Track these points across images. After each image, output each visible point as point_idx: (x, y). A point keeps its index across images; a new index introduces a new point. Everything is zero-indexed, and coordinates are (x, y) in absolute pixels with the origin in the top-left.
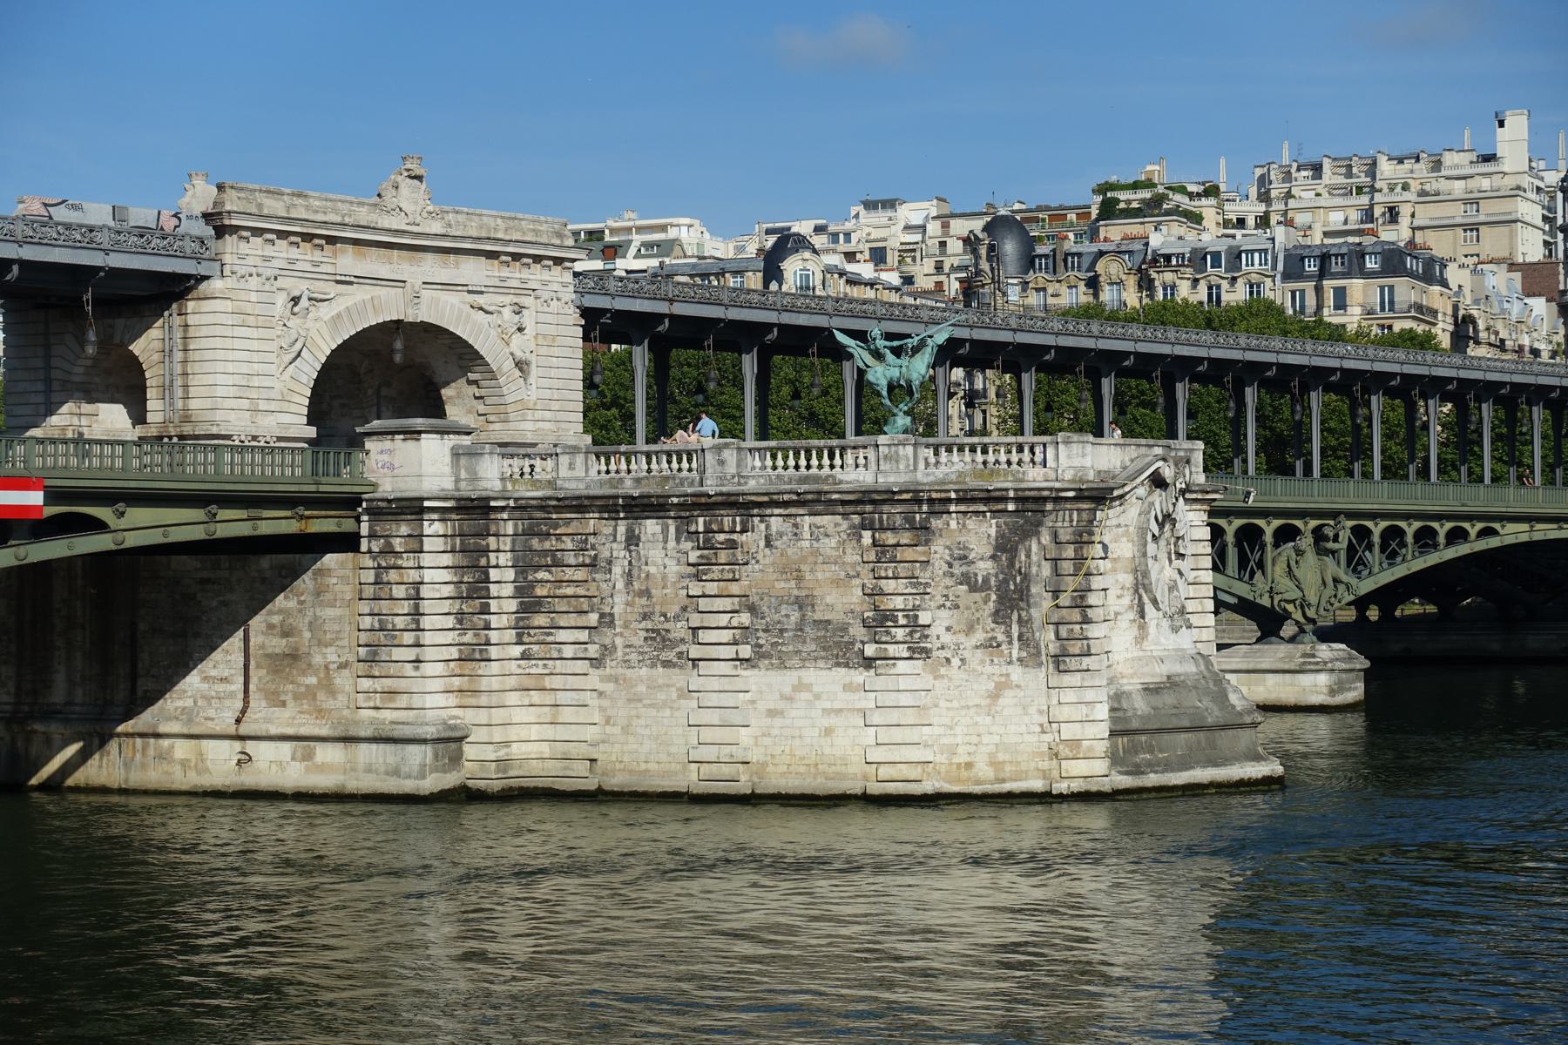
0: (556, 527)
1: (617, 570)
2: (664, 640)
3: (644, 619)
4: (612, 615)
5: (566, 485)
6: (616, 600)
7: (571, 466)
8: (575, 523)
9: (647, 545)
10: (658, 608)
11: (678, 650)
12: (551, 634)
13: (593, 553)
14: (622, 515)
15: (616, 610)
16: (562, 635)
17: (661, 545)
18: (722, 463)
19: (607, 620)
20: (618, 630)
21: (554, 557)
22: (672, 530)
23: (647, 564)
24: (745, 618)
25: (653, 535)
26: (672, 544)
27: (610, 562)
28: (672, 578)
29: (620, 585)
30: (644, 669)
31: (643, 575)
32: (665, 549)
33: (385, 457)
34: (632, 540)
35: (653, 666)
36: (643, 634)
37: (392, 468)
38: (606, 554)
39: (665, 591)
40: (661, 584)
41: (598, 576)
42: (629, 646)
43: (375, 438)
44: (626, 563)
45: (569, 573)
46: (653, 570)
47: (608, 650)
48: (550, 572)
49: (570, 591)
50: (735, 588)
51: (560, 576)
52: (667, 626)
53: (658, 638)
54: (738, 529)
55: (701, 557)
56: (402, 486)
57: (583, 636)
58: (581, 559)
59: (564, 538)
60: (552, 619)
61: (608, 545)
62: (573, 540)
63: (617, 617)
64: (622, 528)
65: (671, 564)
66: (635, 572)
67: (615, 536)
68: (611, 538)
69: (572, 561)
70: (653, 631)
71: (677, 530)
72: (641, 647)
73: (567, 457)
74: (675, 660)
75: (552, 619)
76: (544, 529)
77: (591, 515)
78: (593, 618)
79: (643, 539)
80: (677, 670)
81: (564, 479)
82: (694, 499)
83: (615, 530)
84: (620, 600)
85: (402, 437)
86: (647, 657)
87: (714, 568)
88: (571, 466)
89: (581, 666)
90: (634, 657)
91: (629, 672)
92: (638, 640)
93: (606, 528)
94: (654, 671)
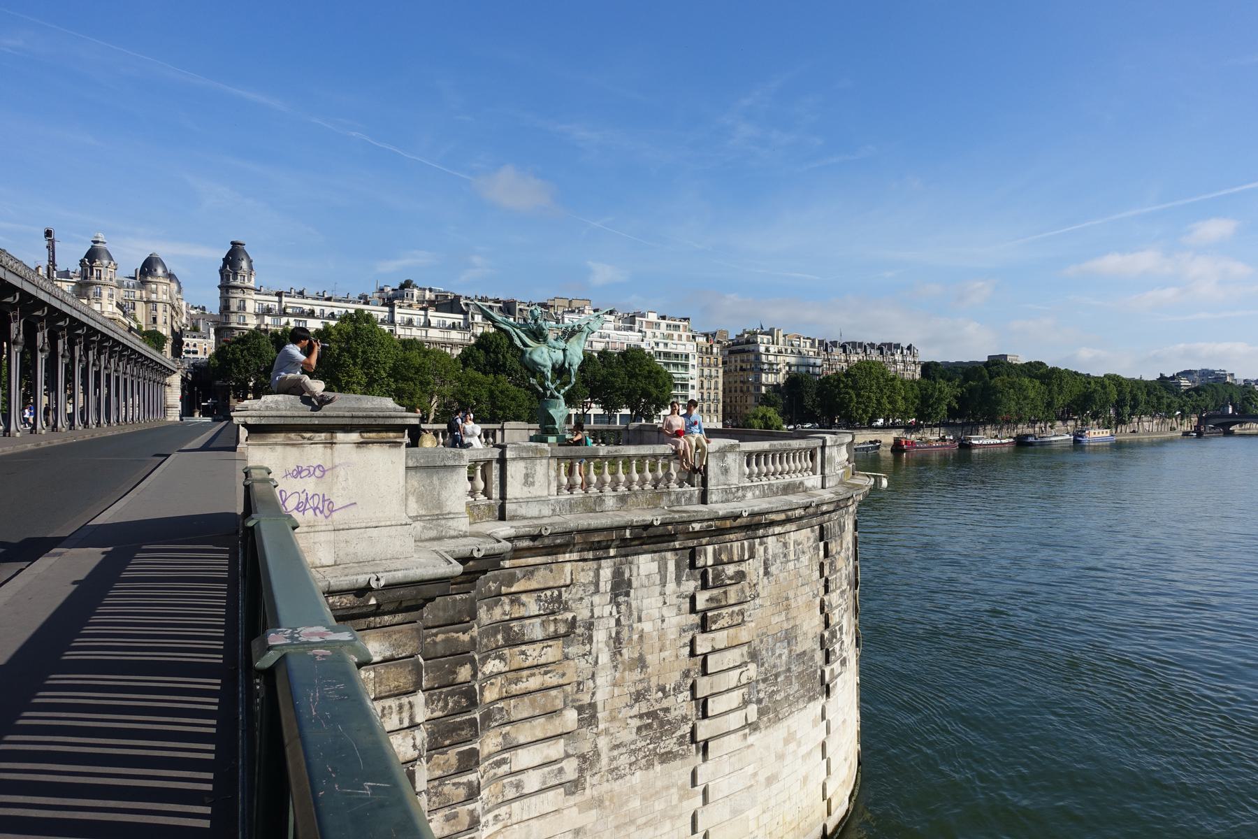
0: (511, 580)
1: (600, 636)
2: (662, 724)
3: (637, 701)
4: (593, 706)
5: (523, 511)
6: (599, 681)
7: (528, 480)
8: (542, 572)
9: (639, 593)
10: (654, 682)
11: (679, 733)
12: (504, 761)
13: (569, 616)
14: (612, 552)
15: (600, 697)
16: (523, 758)
17: (658, 589)
18: (726, 471)
19: (588, 715)
20: (602, 726)
21: (507, 630)
22: (671, 566)
23: (640, 620)
24: (752, 670)
25: (648, 576)
26: (671, 586)
27: (590, 626)
28: (672, 634)
29: (604, 658)
30: (638, 773)
31: (635, 637)
32: (663, 594)
33: (310, 485)
34: (621, 586)
35: (650, 765)
36: (636, 723)
37: (326, 506)
38: (583, 614)
39: (663, 655)
40: (657, 645)
41: (572, 650)
42: (617, 747)
43: (280, 437)
44: (613, 622)
45: (534, 654)
46: (647, 626)
47: (587, 761)
48: (501, 658)
49: (534, 683)
50: (744, 634)
51: (518, 661)
52: (665, 704)
53: (656, 723)
54: (746, 557)
55: (710, 600)
56: (362, 548)
57: (555, 750)
58: (552, 629)
59: (524, 598)
60: (505, 736)
61: (586, 601)
62: (539, 599)
63: (600, 707)
64: (606, 573)
65: (669, 613)
66: (625, 634)
67: (597, 585)
68: (592, 588)
69: (538, 633)
70: (649, 715)
71: (678, 566)
72: (634, 742)
73: (521, 464)
74: (676, 748)
75: (505, 736)
76: (493, 586)
77: (567, 557)
78: (571, 716)
79: (635, 584)
80: (678, 762)
81: (517, 501)
82: (718, 523)
83: (597, 575)
84: (603, 680)
85: (355, 437)
86: (641, 754)
87: (724, 611)
88: (528, 480)
89: (554, 798)
90: (624, 760)
91: (617, 786)
92: (627, 735)
93: (586, 577)
94: (651, 772)
